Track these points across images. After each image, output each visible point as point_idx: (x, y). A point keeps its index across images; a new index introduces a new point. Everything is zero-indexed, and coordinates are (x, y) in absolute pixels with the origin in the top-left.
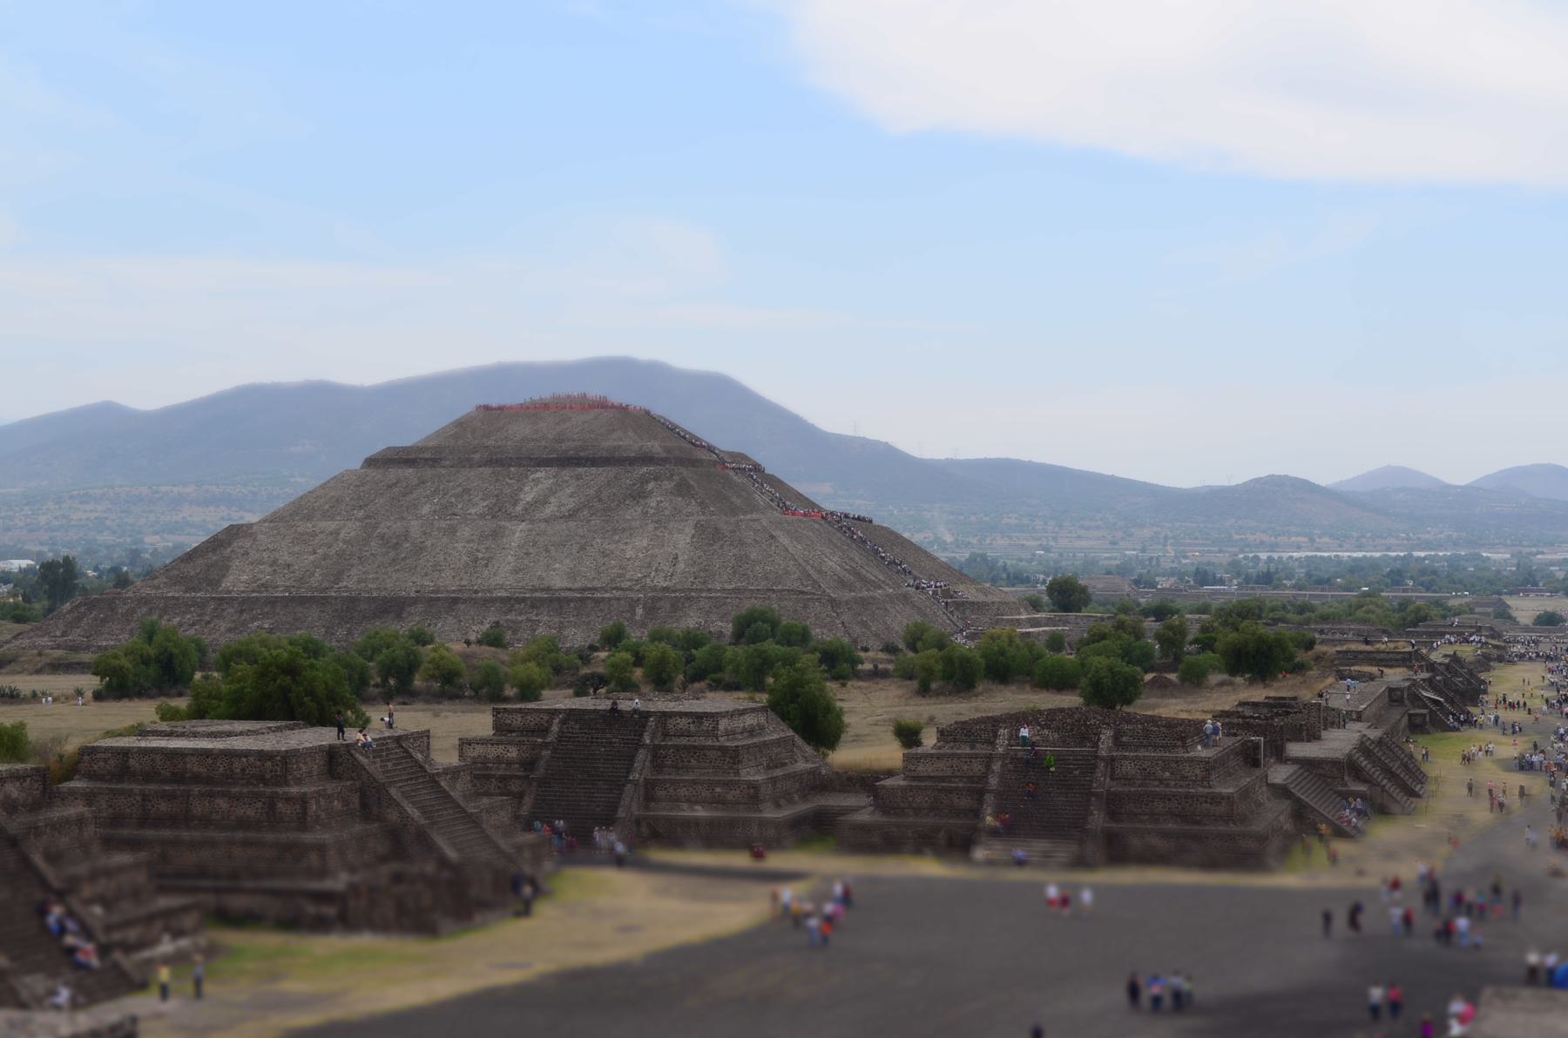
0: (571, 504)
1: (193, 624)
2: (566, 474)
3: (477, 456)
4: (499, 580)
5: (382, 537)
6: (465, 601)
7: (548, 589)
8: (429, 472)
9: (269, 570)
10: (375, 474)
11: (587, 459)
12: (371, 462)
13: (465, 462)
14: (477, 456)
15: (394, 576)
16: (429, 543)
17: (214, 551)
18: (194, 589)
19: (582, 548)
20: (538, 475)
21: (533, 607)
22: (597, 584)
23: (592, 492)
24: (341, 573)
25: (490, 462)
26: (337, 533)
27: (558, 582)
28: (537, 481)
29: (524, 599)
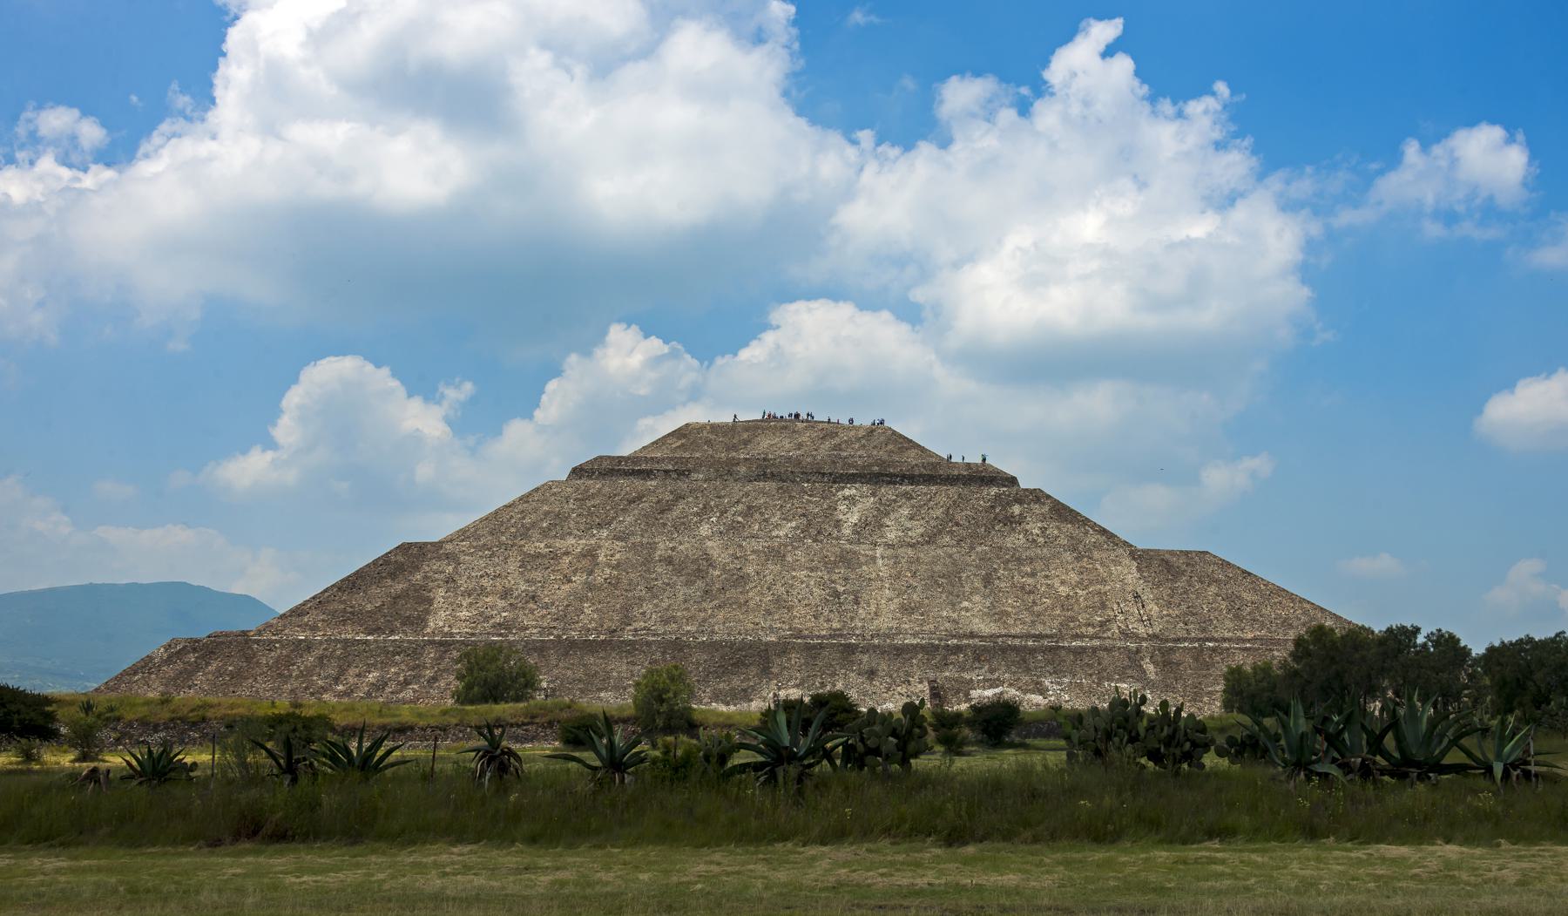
0: (918, 530)
1: (407, 683)
2: (887, 492)
3: (743, 470)
4: (885, 623)
5: (669, 561)
6: (865, 650)
7: (972, 635)
8: (683, 485)
9: (501, 604)
10: (595, 485)
11: (904, 477)
12: (578, 472)
13: (726, 471)
14: (743, 470)
15: (721, 615)
16: (750, 570)
17: (393, 576)
18: (377, 630)
19: (987, 581)
20: (847, 492)
21: (977, 659)
22: (1039, 629)
23: (939, 512)
24: (626, 609)
25: (763, 476)
26: (590, 554)
27: (986, 627)
28: (852, 500)
29: (958, 649)
